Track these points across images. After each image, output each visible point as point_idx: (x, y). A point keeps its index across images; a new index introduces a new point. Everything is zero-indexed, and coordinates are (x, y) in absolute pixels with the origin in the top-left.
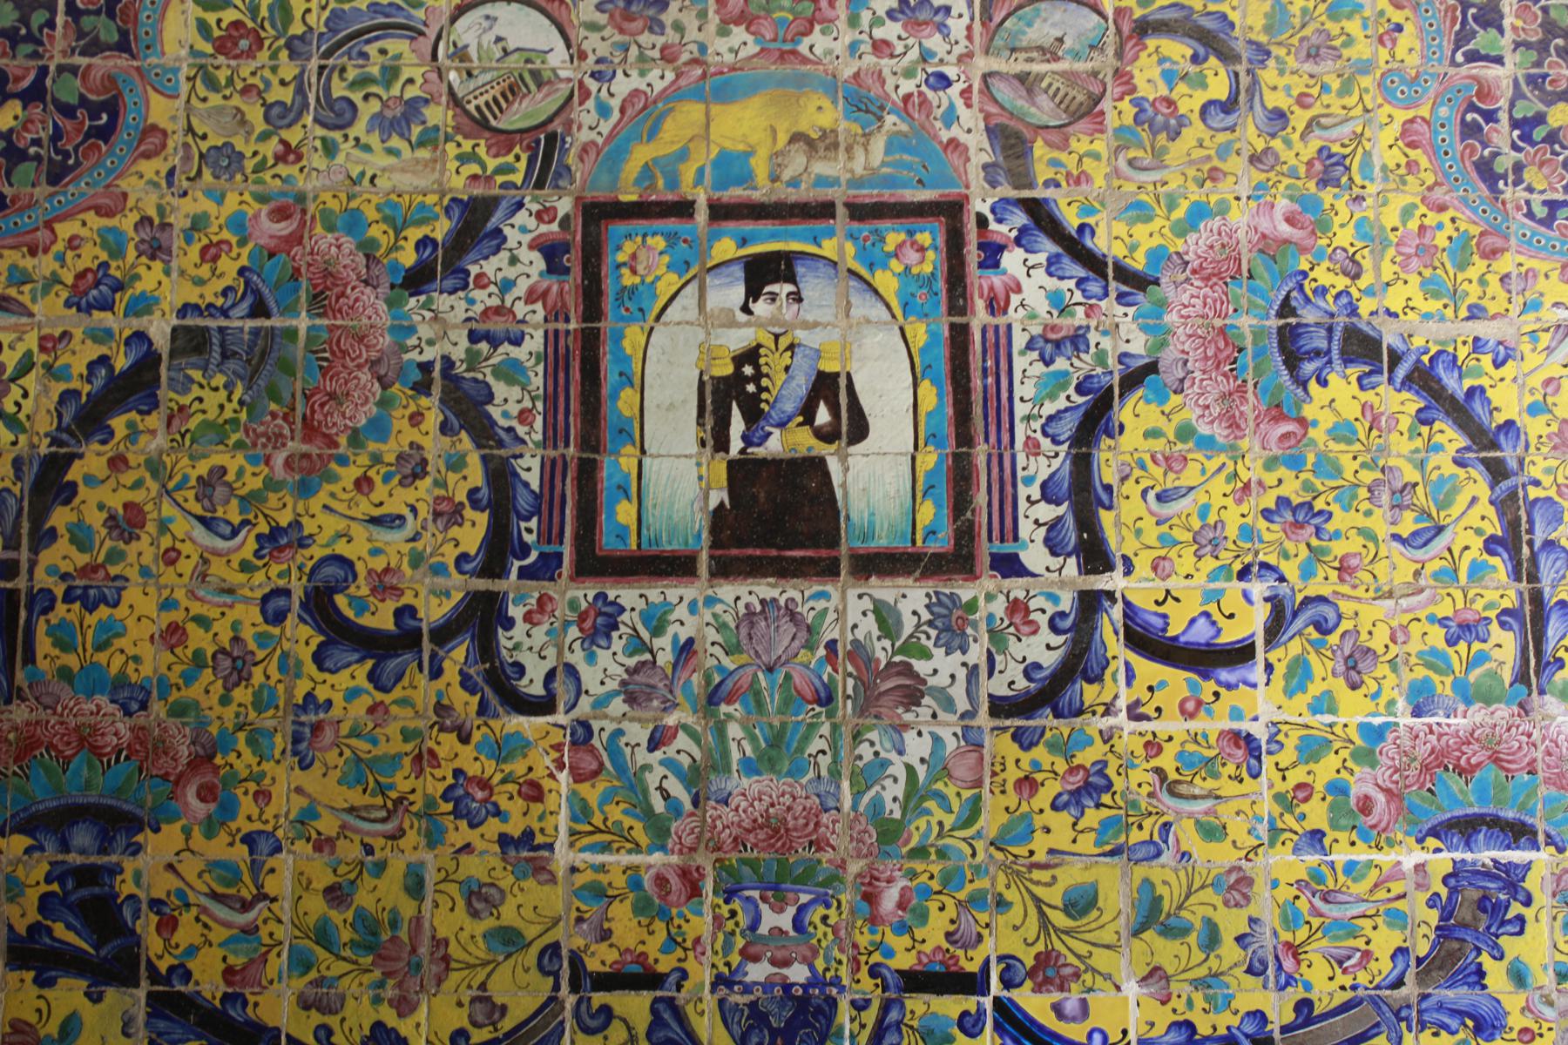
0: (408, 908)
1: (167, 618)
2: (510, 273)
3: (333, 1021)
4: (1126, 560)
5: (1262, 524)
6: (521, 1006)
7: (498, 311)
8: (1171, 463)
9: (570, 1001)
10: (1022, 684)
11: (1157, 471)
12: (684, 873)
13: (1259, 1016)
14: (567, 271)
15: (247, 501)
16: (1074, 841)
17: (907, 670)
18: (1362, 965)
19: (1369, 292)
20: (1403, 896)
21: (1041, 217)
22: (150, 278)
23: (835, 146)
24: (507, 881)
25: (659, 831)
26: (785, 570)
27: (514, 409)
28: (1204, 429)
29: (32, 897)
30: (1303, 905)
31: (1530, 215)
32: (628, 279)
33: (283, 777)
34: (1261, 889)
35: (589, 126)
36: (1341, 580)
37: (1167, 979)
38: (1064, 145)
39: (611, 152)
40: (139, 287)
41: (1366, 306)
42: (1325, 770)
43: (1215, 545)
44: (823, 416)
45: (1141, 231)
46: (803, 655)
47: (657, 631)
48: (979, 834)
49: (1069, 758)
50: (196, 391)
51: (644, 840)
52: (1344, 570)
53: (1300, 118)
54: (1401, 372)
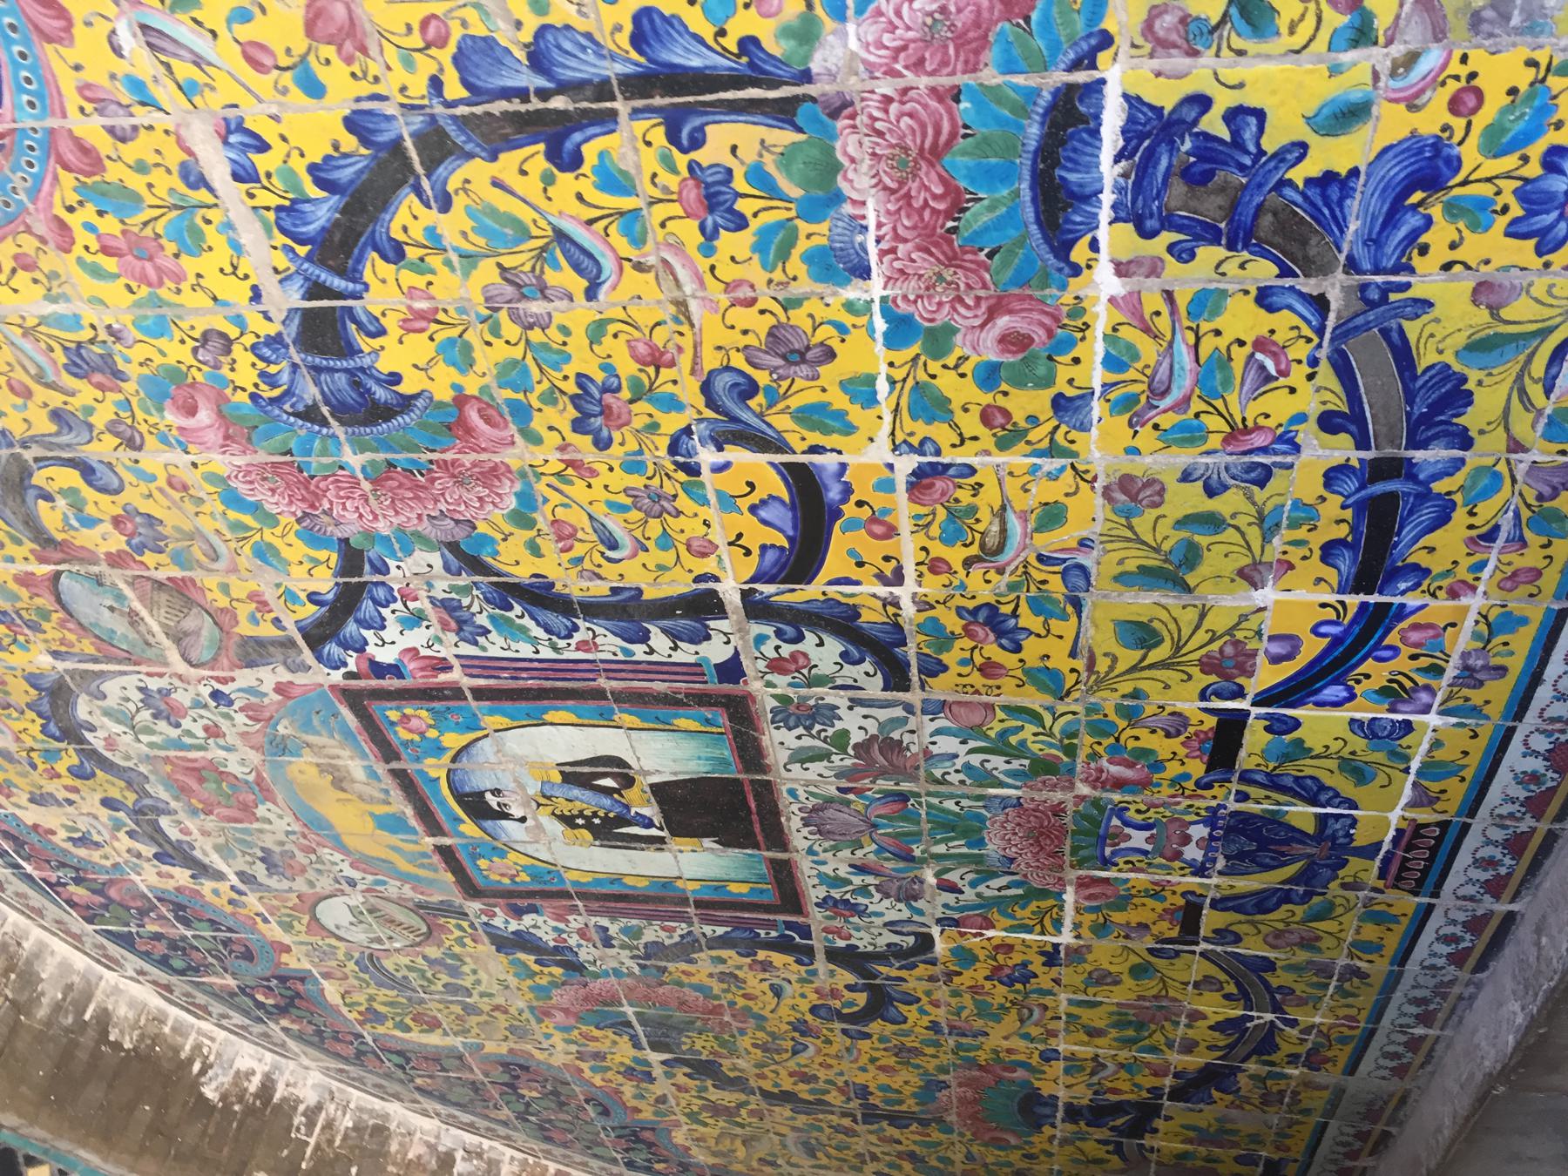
5: (615, 449)
13: (1332, 477)
16: (1061, 637)
18: (1277, 352)
20: (1169, 296)
28: (512, 503)
30: (1167, 421)
34: (1139, 467)
36: (672, 364)
37: (1255, 565)
42: (960, 390)
48: (1051, 709)
49: (954, 637)
52: (657, 359)
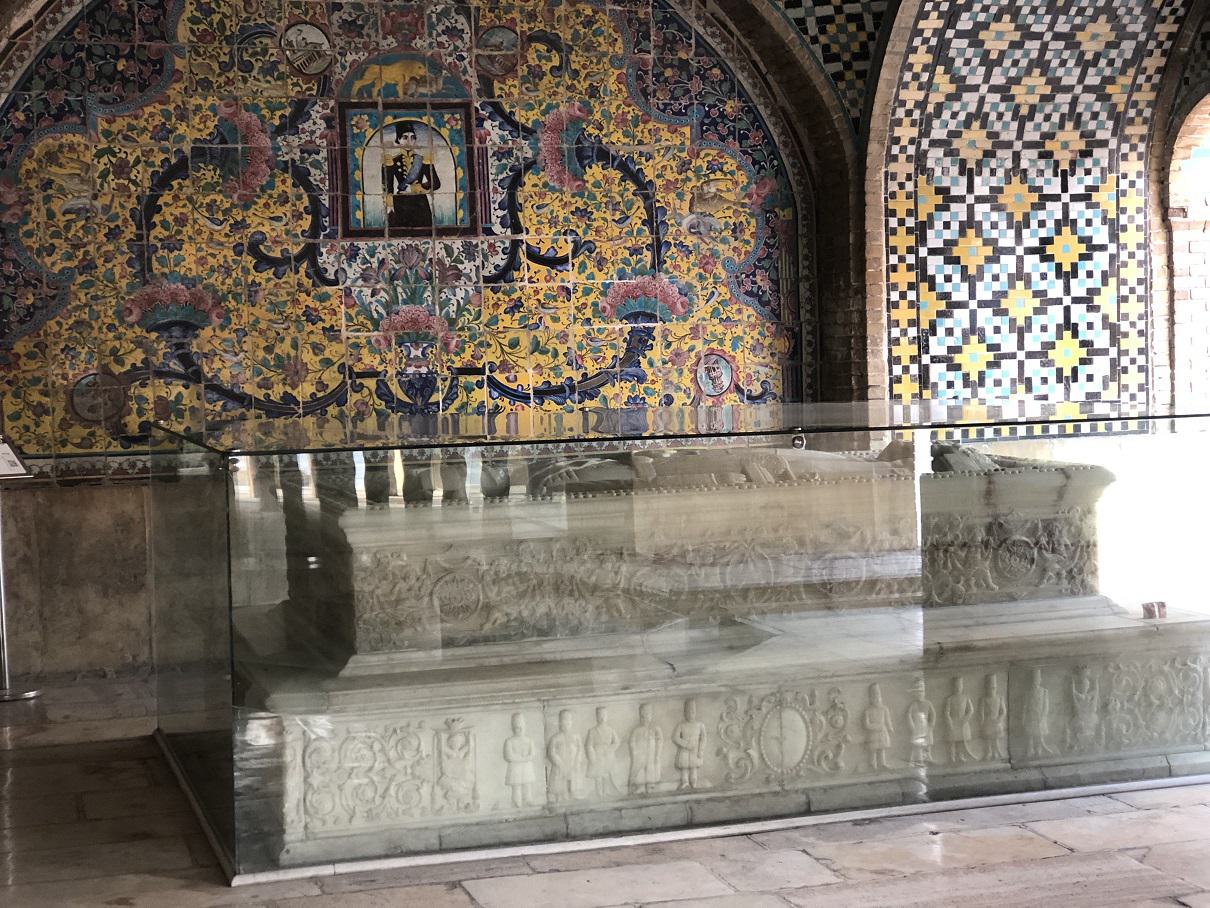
0: (293, 353)
1: (200, 254)
2: (313, 128)
3: (270, 392)
4: (527, 229)
6: (333, 386)
7: (311, 142)
8: (542, 196)
9: (349, 381)
10: (494, 271)
11: (536, 199)
12: (385, 338)
13: (571, 379)
14: (333, 127)
15: (226, 212)
17: (457, 268)
19: (605, 136)
21: (497, 110)
22: (182, 129)
23: (426, 82)
24: (326, 343)
25: (376, 325)
26: (414, 235)
27: (318, 178)
28: (552, 184)
29: (161, 353)
30: (584, 343)
31: (658, 108)
32: (356, 131)
33: (245, 309)
34: (571, 337)
35: (339, 73)
37: (542, 367)
38: (504, 83)
39: (348, 84)
40: (178, 132)
41: (605, 140)
42: (591, 298)
43: (556, 224)
44: (425, 180)
45: (530, 113)
46: (422, 264)
47: (372, 256)
50: (202, 171)
51: (371, 328)
52: (597, 231)
53: (583, 73)
54: (616, 163)
